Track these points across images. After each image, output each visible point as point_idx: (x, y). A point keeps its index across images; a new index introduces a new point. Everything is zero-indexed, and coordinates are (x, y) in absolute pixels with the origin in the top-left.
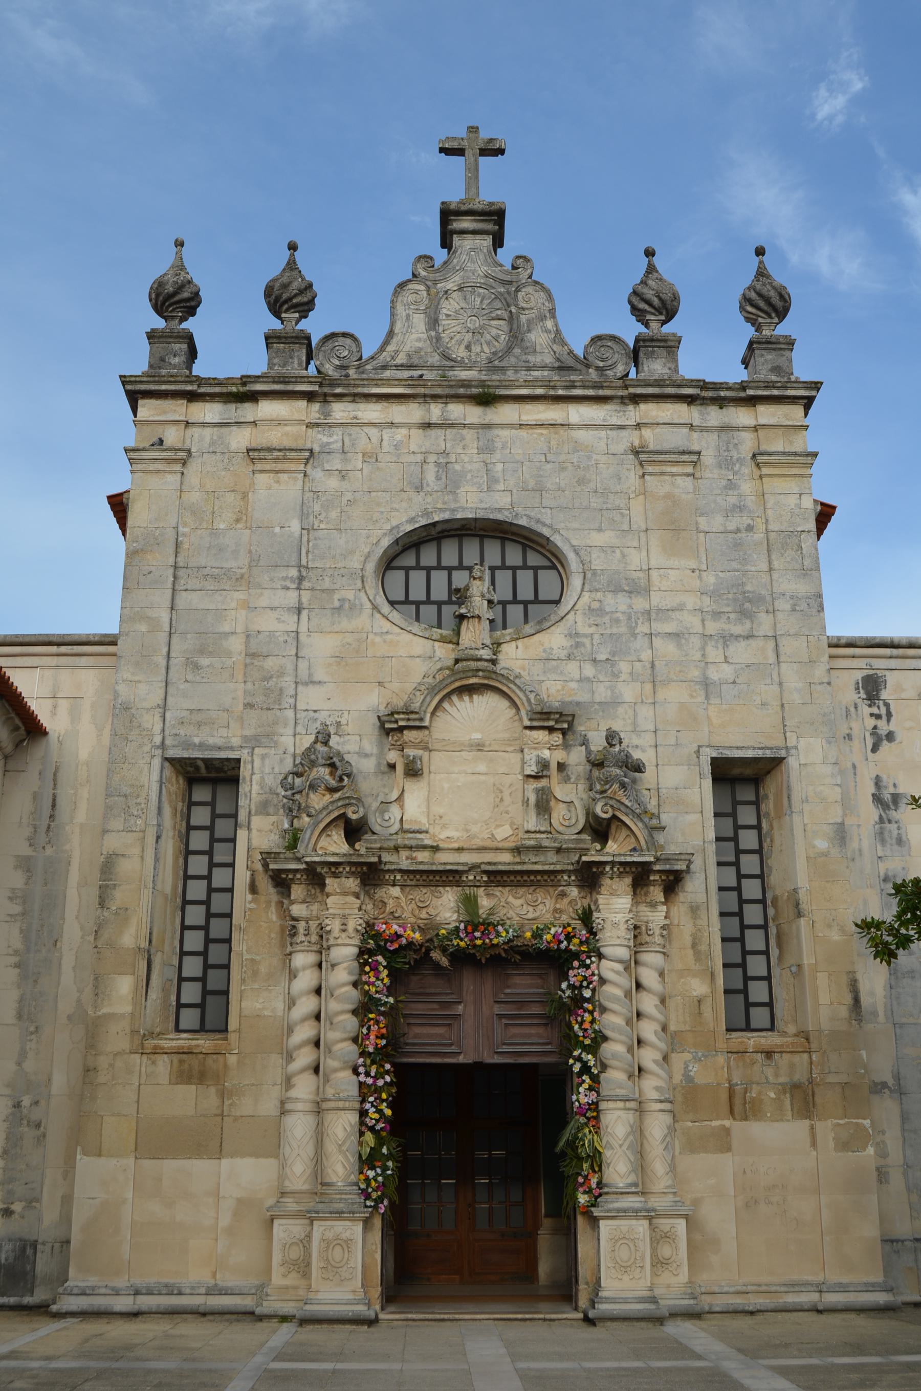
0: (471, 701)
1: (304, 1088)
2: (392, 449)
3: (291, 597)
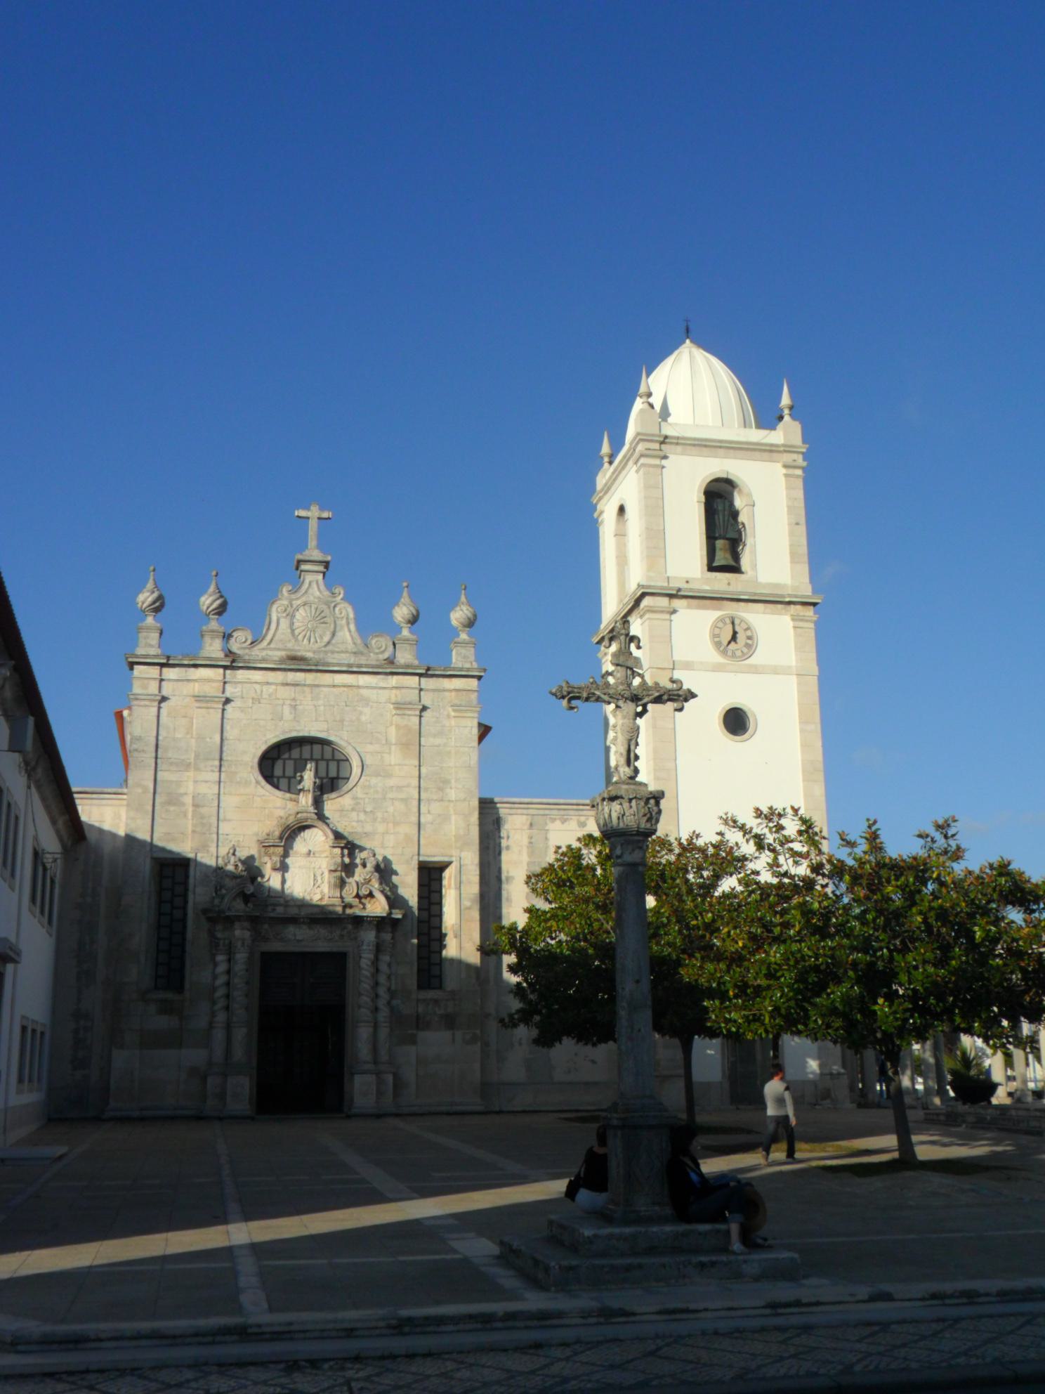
1: (221, 1017)
2: (267, 697)
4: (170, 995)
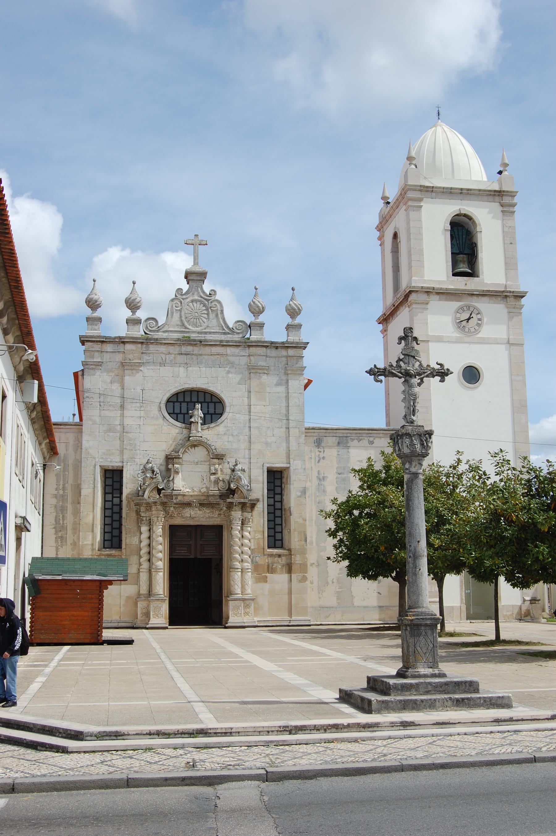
0: (195, 449)
2: (169, 362)
3: (137, 414)
4: (113, 552)
